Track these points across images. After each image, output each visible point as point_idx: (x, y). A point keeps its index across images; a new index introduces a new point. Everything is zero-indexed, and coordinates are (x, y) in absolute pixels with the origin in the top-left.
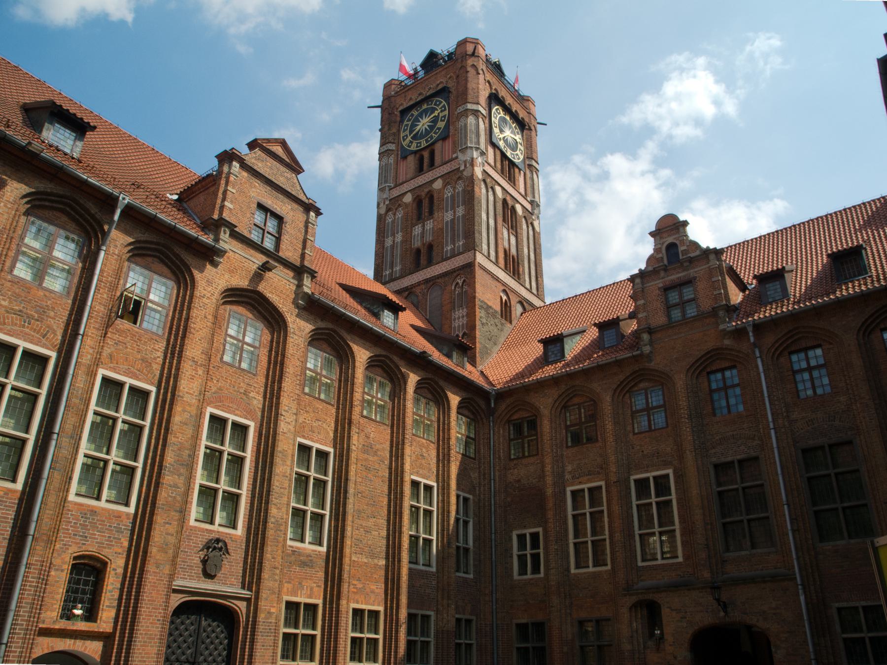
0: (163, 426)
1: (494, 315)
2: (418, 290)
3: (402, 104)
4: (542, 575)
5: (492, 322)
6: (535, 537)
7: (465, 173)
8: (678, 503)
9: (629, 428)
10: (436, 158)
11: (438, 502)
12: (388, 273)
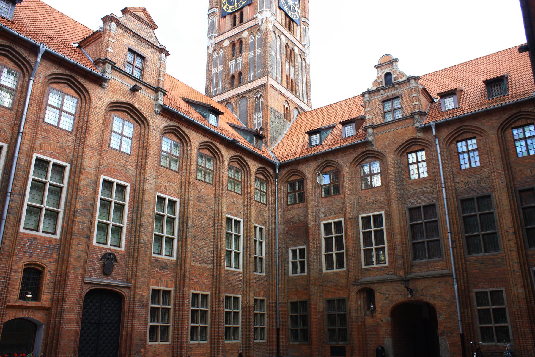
0: (74, 186)
1: (279, 117)
2: (232, 101)
4: (306, 274)
5: (278, 121)
6: (302, 251)
7: (262, 27)
8: (387, 231)
9: (359, 186)
10: (244, 17)
11: (243, 231)
12: (214, 90)
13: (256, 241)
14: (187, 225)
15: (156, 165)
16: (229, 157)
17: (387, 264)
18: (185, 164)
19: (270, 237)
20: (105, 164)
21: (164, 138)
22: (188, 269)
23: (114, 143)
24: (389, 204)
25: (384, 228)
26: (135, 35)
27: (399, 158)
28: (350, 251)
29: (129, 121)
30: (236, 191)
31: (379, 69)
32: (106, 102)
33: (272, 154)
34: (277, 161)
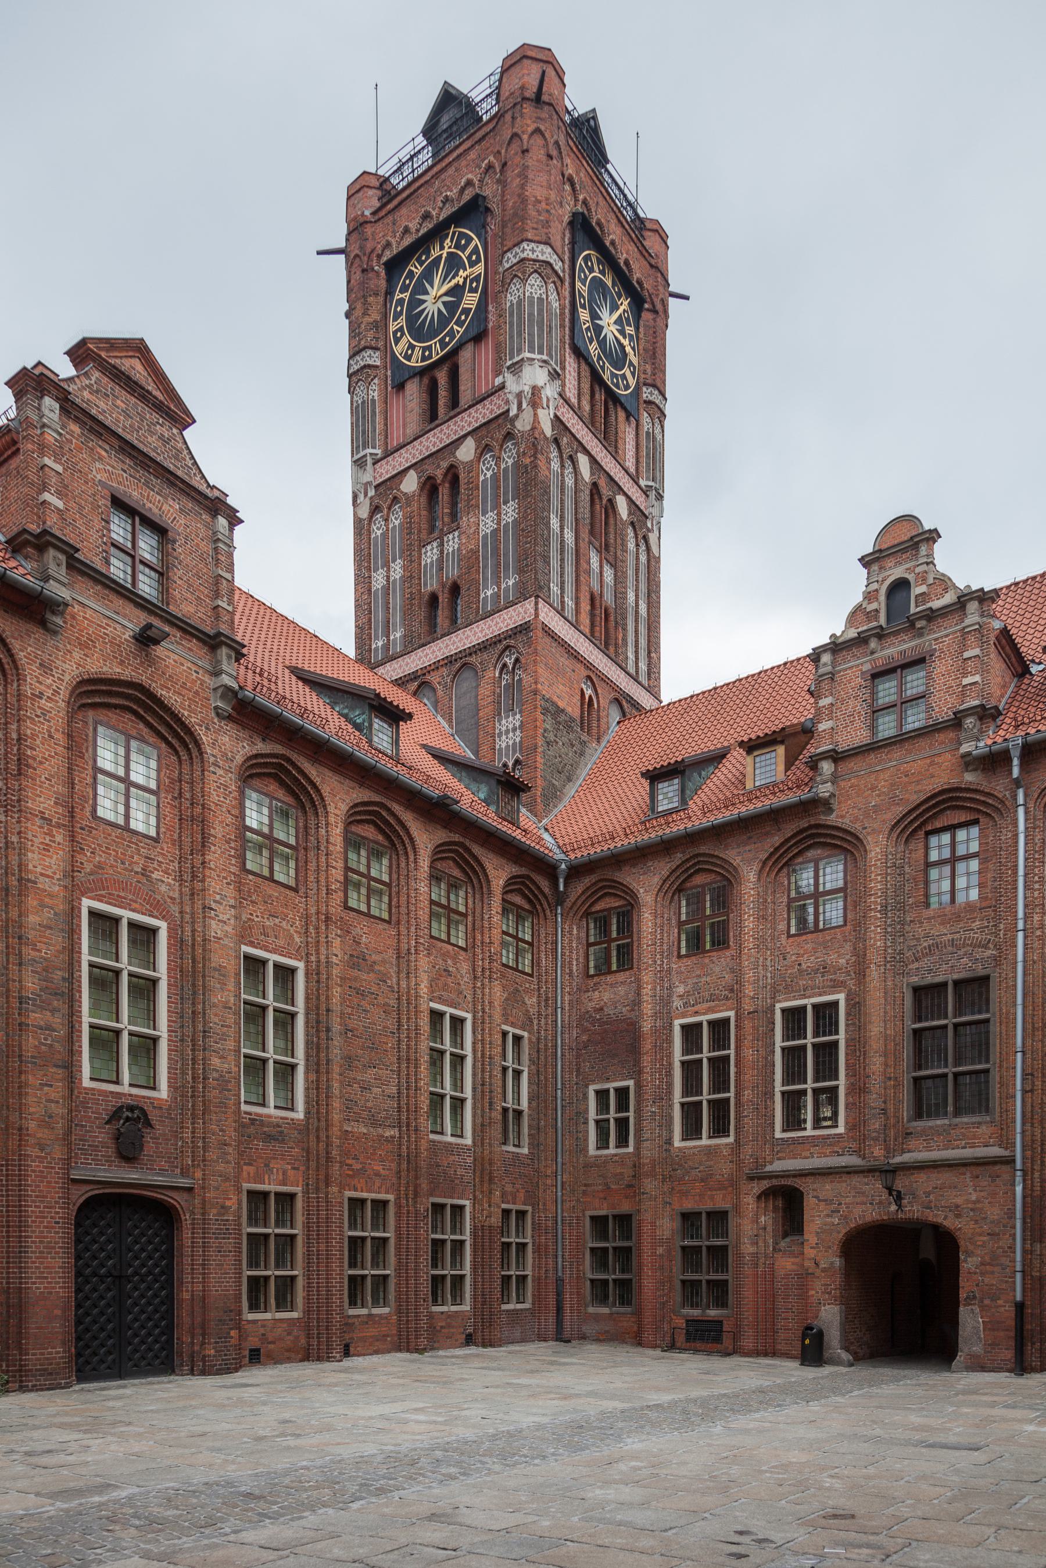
3: (388, 245)
4: (631, 1149)
9: (782, 926)
10: (462, 388)
13: (505, 1069)
14: (328, 1030)
15: (233, 869)
16: (430, 846)
17: (841, 1129)
18: (312, 866)
19: (542, 1058)
20: (88, 867)
21: (248, 792)
22: (336, 1141)
23: (108, 807)
24: (861, 972)
25: (842, 1037)
26: (127, 449)
27: (901, 848)
28: (747, 1094)
29: (142, 739)
30: (453, 940)
31: (875, 567)
32: (67, 678)
33: (546, 836)
34: (562, 856)
